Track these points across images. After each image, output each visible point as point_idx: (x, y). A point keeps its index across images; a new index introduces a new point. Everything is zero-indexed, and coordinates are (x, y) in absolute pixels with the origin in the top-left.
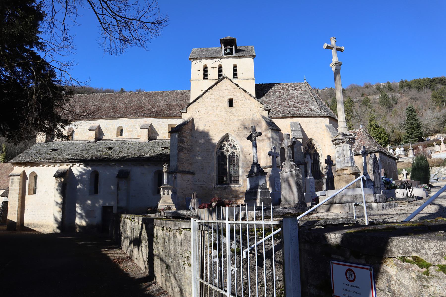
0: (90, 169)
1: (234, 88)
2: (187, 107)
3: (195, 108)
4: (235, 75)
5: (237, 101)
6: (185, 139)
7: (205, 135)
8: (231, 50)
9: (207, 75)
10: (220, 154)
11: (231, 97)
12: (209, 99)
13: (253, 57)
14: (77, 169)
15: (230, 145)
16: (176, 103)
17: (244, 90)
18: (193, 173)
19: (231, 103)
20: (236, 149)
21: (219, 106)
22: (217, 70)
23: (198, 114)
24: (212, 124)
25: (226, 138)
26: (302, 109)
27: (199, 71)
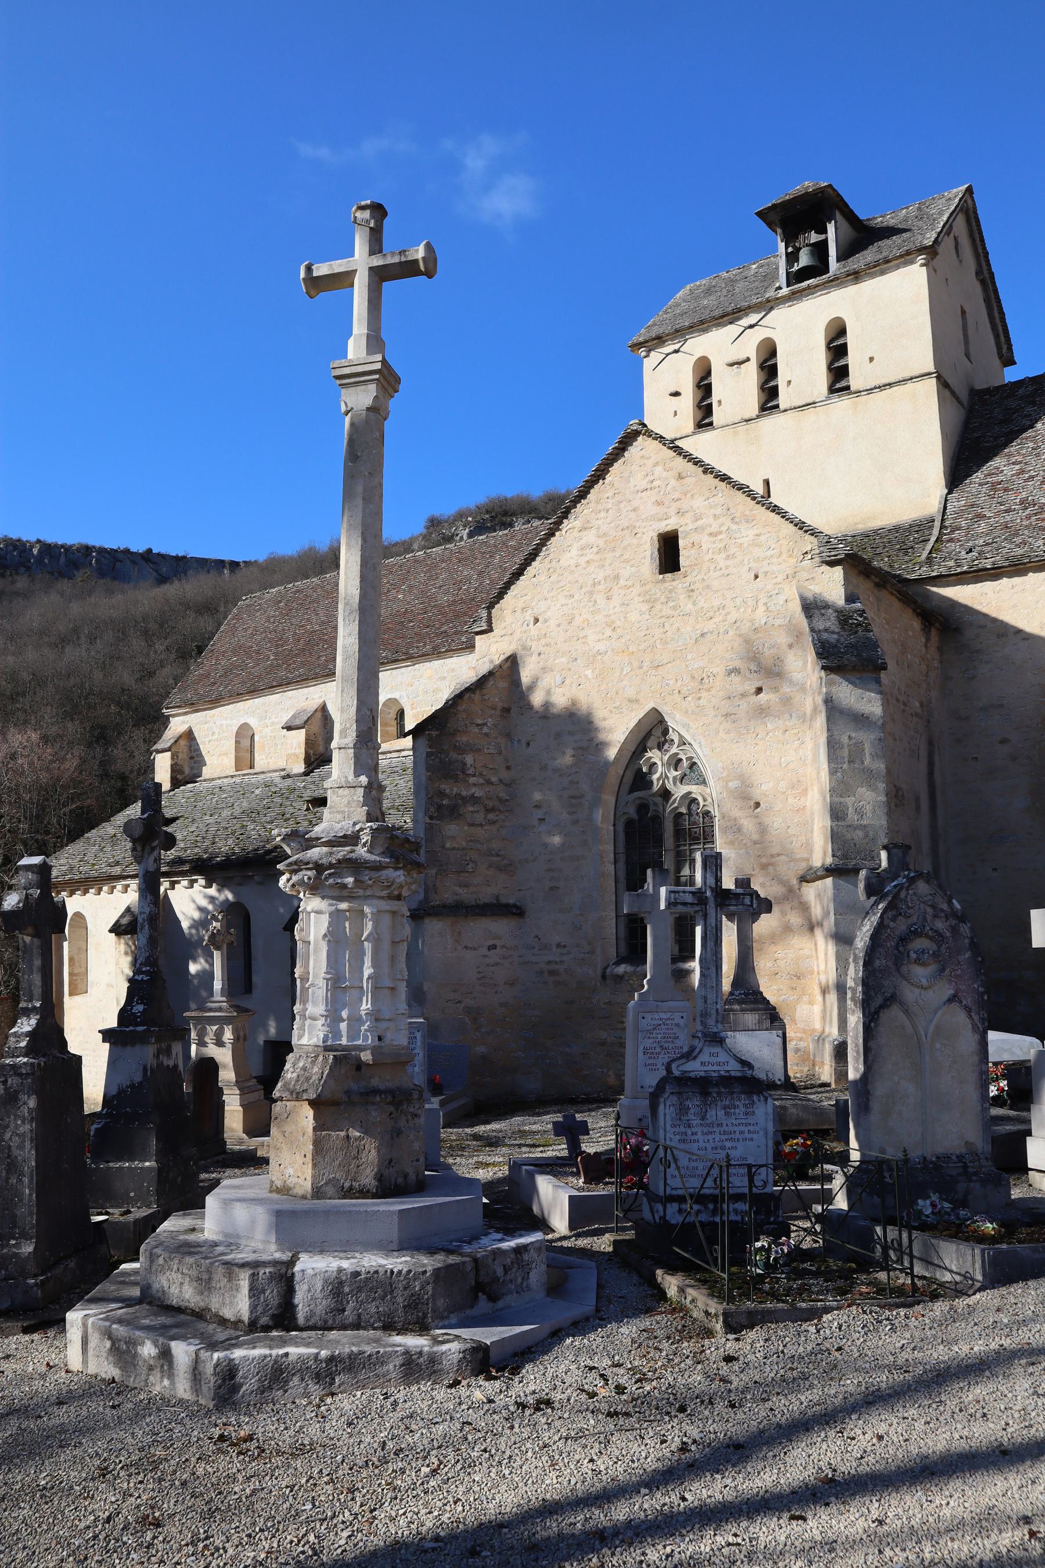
0: (230, 896)
1: (680, 477)
2: (490, 607)
3: (520, 604)
4: (838, 375)
5: (695, 537)
6: (469, 759)
7: (576, 726)
8: (820, 250)
9: (708, 411)
10: (632, 812)
11: (666, 526)
12: (574, 552)
13: (921, 259)
14: (189, 900)
15: (677, 763)
17: (724, 478)
18: (515, 911)
19: (669, 553)
20: (704, 782)
21: (617, 577)
22: (751, 373)
23: (534, 630)
24: (589, 673)
25: (653, 730)
27: (676, 394)
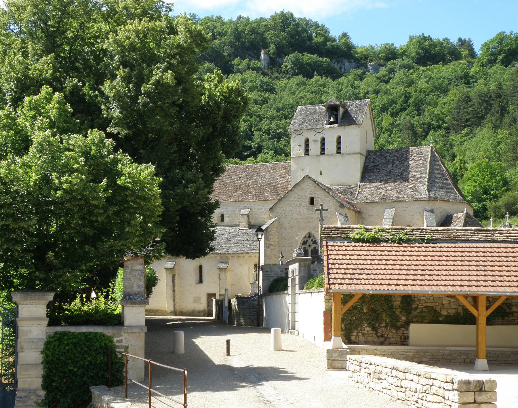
4: (339, 148)
6: (271, 237)
12: (293, 198)
16: (278, 181)
19: (312, 201)
21: (301, 204)
22: (319, 145)
23: (284, 212)
26: (408, 189)
